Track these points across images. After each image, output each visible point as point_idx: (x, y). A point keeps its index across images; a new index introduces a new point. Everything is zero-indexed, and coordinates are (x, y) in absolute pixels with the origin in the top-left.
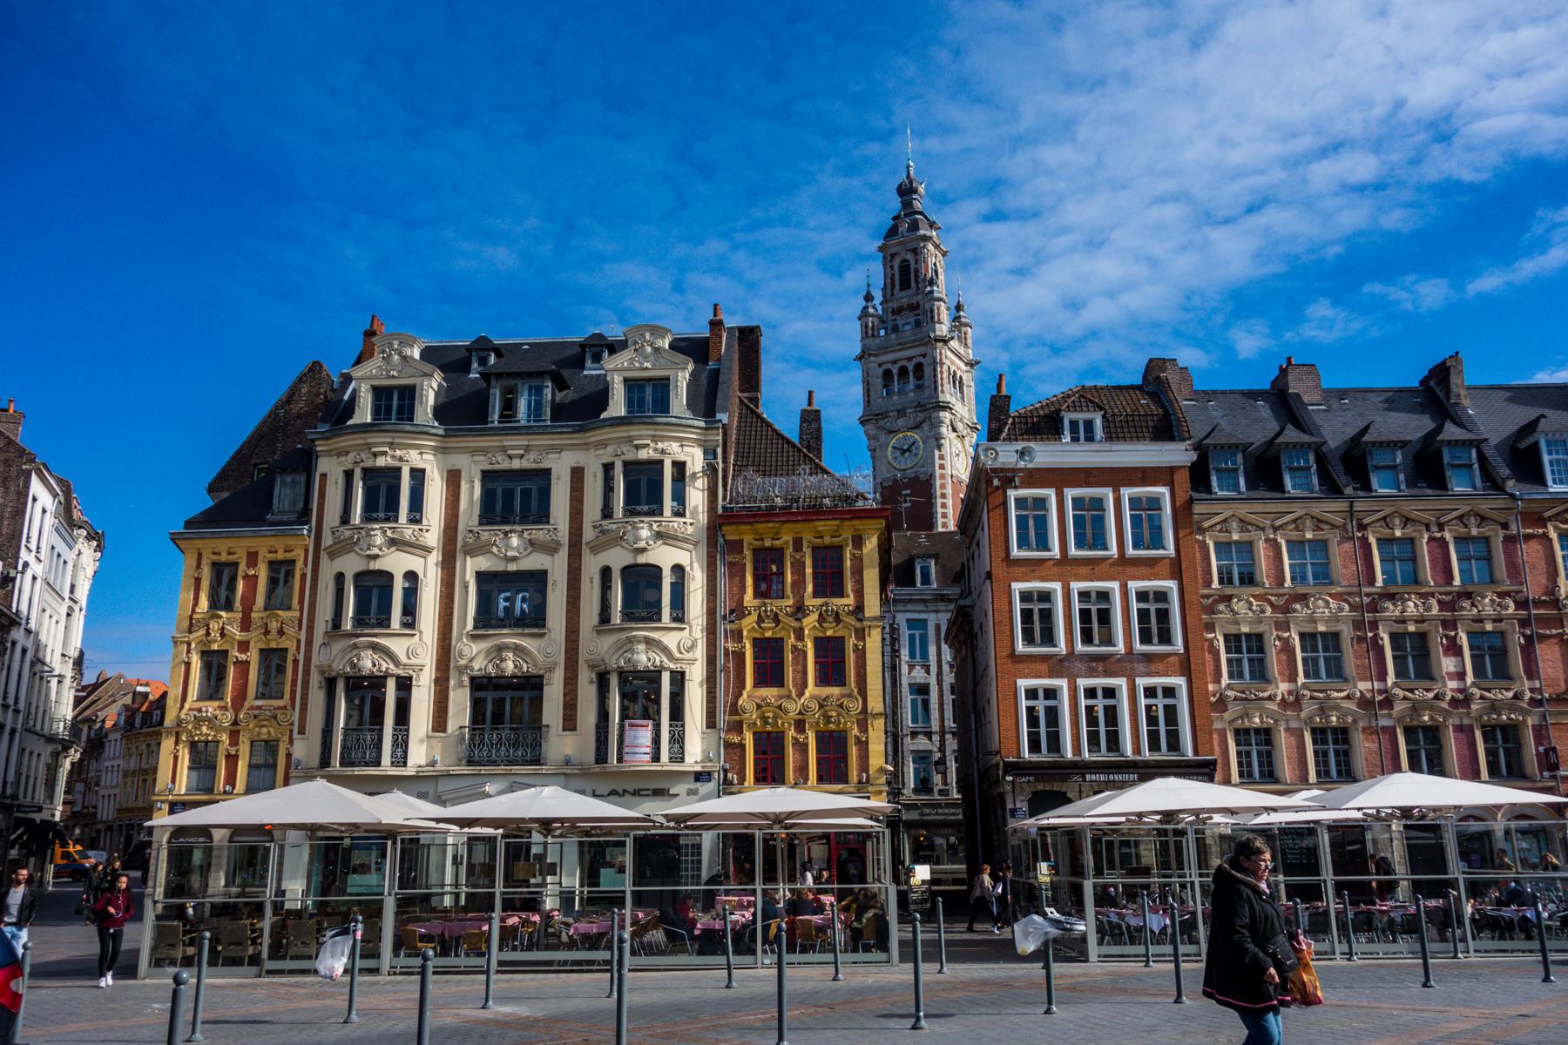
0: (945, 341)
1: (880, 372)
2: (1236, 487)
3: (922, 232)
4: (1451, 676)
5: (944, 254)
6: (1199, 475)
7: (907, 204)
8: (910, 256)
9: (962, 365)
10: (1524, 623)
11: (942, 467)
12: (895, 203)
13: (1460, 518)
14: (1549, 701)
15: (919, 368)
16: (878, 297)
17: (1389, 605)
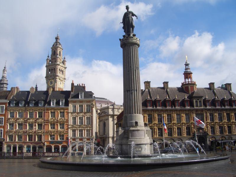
0: (59, 65)
1: (49, 69)
2: (13, 105)
3: (57, 46)
4: (34, 129)
5: (62, 49)
6: (9, 103)
7: (57, 40)
8: (55, 50)
9: (64, 68)
10: (44, 123)
11: (56, 86)
12: (55, 41)
13: (39, 109)
14: (45, 132)
15: (54, 69)
16: (50, 56)
17: (28, 120)
